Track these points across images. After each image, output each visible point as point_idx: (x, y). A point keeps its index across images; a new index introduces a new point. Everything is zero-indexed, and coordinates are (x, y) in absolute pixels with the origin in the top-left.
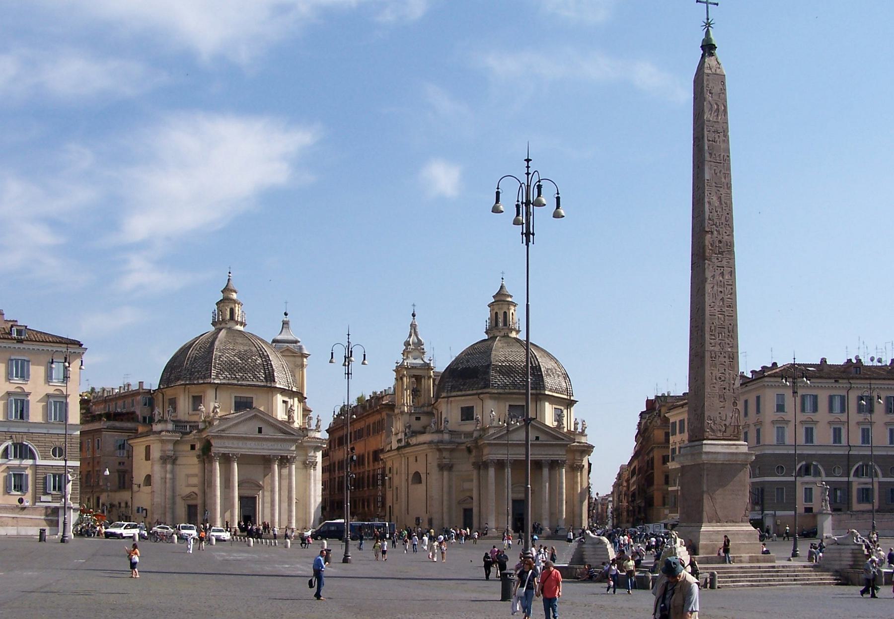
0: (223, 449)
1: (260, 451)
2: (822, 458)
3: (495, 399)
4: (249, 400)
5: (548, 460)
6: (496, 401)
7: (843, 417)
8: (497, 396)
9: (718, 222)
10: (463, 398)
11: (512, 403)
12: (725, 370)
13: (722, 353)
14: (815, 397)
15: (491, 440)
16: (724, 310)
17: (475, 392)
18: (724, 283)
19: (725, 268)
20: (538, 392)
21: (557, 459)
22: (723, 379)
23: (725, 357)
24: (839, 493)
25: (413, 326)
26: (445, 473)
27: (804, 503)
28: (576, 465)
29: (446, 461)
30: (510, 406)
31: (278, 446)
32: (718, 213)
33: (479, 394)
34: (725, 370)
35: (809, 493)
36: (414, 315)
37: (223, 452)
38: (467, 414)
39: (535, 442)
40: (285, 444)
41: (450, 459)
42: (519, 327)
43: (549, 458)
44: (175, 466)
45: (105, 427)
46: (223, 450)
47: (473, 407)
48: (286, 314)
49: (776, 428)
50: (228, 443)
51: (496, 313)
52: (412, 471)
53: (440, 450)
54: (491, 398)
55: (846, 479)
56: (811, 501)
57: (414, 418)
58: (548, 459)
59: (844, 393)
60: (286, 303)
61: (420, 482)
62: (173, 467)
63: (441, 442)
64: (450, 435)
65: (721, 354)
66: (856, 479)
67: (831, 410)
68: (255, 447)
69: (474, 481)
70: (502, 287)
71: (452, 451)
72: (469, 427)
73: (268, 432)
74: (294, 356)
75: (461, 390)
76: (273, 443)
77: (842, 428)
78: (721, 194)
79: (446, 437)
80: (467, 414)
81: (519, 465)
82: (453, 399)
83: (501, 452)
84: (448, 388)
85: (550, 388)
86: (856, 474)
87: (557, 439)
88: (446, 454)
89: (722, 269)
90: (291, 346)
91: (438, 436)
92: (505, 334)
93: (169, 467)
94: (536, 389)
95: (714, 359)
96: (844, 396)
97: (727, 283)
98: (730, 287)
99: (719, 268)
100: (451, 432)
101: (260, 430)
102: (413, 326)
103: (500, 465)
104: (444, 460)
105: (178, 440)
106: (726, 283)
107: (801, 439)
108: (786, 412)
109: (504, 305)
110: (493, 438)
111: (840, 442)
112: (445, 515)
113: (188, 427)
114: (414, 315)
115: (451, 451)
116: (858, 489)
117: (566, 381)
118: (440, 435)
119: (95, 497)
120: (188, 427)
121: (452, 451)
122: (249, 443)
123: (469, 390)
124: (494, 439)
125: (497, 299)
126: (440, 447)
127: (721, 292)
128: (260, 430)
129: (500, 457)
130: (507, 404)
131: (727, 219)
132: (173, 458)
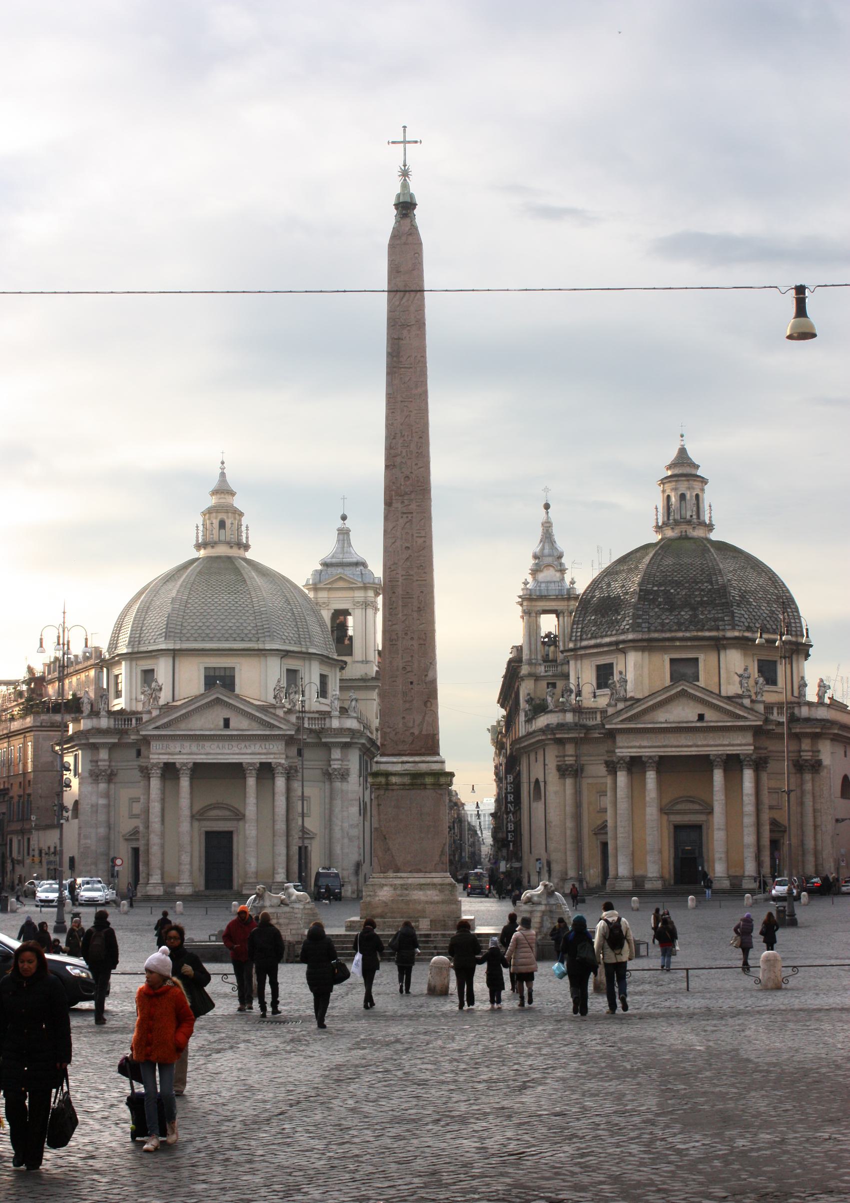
0: (166, 757)
1: (227, 757)
3: (643, 649)
4: (228, 673)
5: (722, 755)
6: (646, 654)
8: (645, 644)
9: (404, 451)
10: (595, 651)
12: (412, 656)
13: (409, 633)
15: (615, 724)
16: (412, 573)
17: (613, 639)
18: (412, 535)
19: (414, 514)
20: (721, 634)
21: (738, 752)
22: (409, 669)
23: (412, 638)
25: (547, 527)
26: (569, 782)
28: (804, 760)
29: (570, 760)
30: (672, 661)
31: (256, 747)
32: (406, 438)
33: (617, 643)
34: (412, 656)
36: (547, 507)
37: (165, 761)
38: (604, 675)
39: (693, 725)
40: (267, 744)
41: (576, 756)
42: (710, 517)
43: (721, 750)
44: (112, 786)
45: (39, 724)
46: (165, 758)
47: (613, 664)
48: (344, 518)
50: (176, 746)
51: (668, 497)
52: (533, 780)
53: (560, 742)
54: (636, 649)
57: (544, 684)
58: (720, 753)
60: (344, 499)
61: (540, 799)
62: (109, 788)
63: (561, 726)
64: (577, 714)
65: (406, 634)
68: (218, 751)
69: (609, 794)
70: (682, 451)
71: (576, 741)
72: (603, 702)
73: (239, 724)
74: (351, 589)
75: (594, 637)
76: (247, 743)
78: (410, 411)
79: (569, 717)
80: (604, 675)
81: (665, 764)
82: (583, 652)
83: (637, 744)
84: (577, 632)
85: (746, 624)
87: (736, 718)
88: (570, 749)
89: (410, 516)
90: (348, 572)
91: (558, 717)
92: (681, 532)
93: (103, 786)
94: (718, 629)
95: (394, 642)
97: (417, 535)
98: (423, 539)
99: (405, 516)
100: (578, 710)
102: (547, 527)
103: (635, 765)
104: (566, 758)
105: (115, 743)
106: (416, 535)
109: (680, 483)
110: (621, 718)
112: (568, 853)
113: (134, 721)
114: (547, 507)
115: (576, 743)
117: (789, 610)
118: (560, 715)
119: (26, 840)
120: (134, 721)
121: (576, 741)
122: (207, 744)
123: (606, 636)
124: (621, 721)
125: (677, 471)
126: (558, 736)
127: (407, 548)
129: (634, 752)
130: (667, 658)
131: (419, 445)
132: (109, 772)
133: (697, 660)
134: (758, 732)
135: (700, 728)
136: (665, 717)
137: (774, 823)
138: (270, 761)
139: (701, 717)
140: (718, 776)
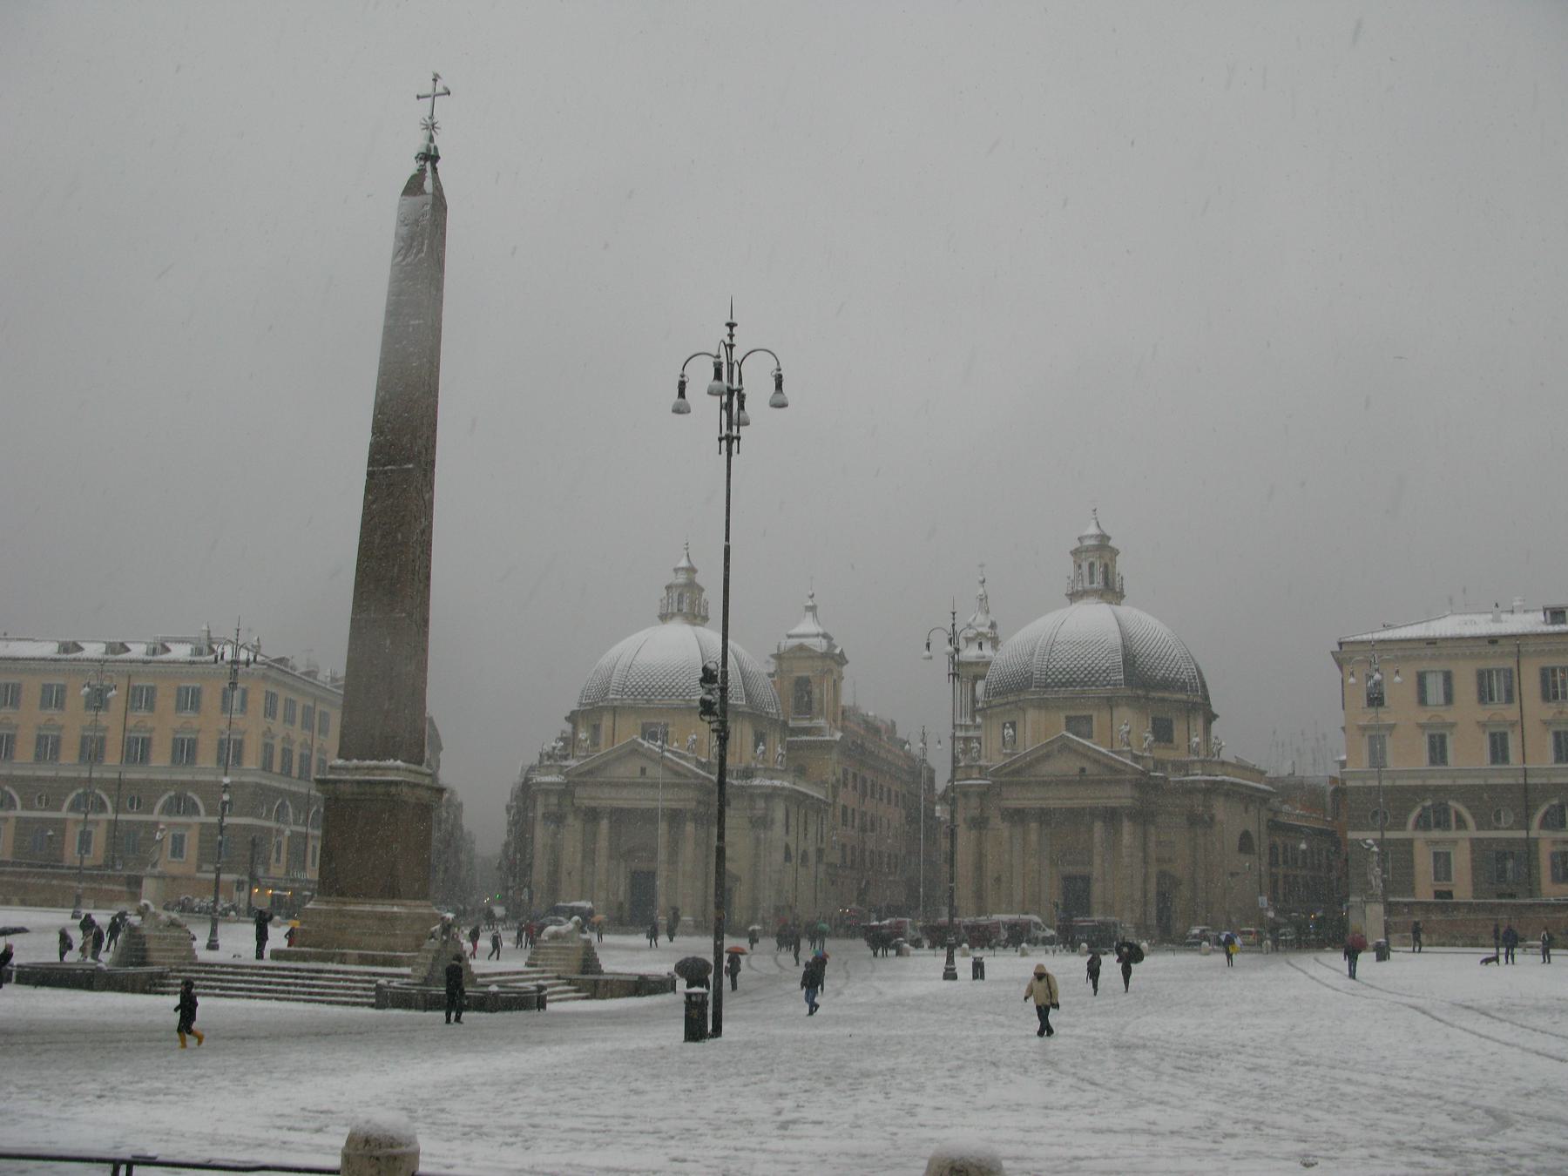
2: (1469, 794)
7: (1512, 712)
11: (1072, 713)
14: (1448, 677)
24: (1510, 864)
27: (1433, 882)
30: (1067, 718)
35: (1442, 863)
49: (1366, 738)
55: (1522, 834)
56: (1448, 877)
59: (1510, 663)
66: (1545, 834)
67: (1485, 696)
77: (1448, 734)
81: (1044, 816)
86: (1544, 824)
96: (1511, 671)
101: (643, 771)
107: (1422, 760)
108: (1388, 707)
111: (1505, 759)
116: (1553, 855)
128: (643, 771)
133: (1090, 718)
134: (1137, 785)
135: (1082, 778)
136: (1049, 769)
137: (1162, 875)
138: (680, 807)
139: (1083, 770)
140: (1098, 826)
